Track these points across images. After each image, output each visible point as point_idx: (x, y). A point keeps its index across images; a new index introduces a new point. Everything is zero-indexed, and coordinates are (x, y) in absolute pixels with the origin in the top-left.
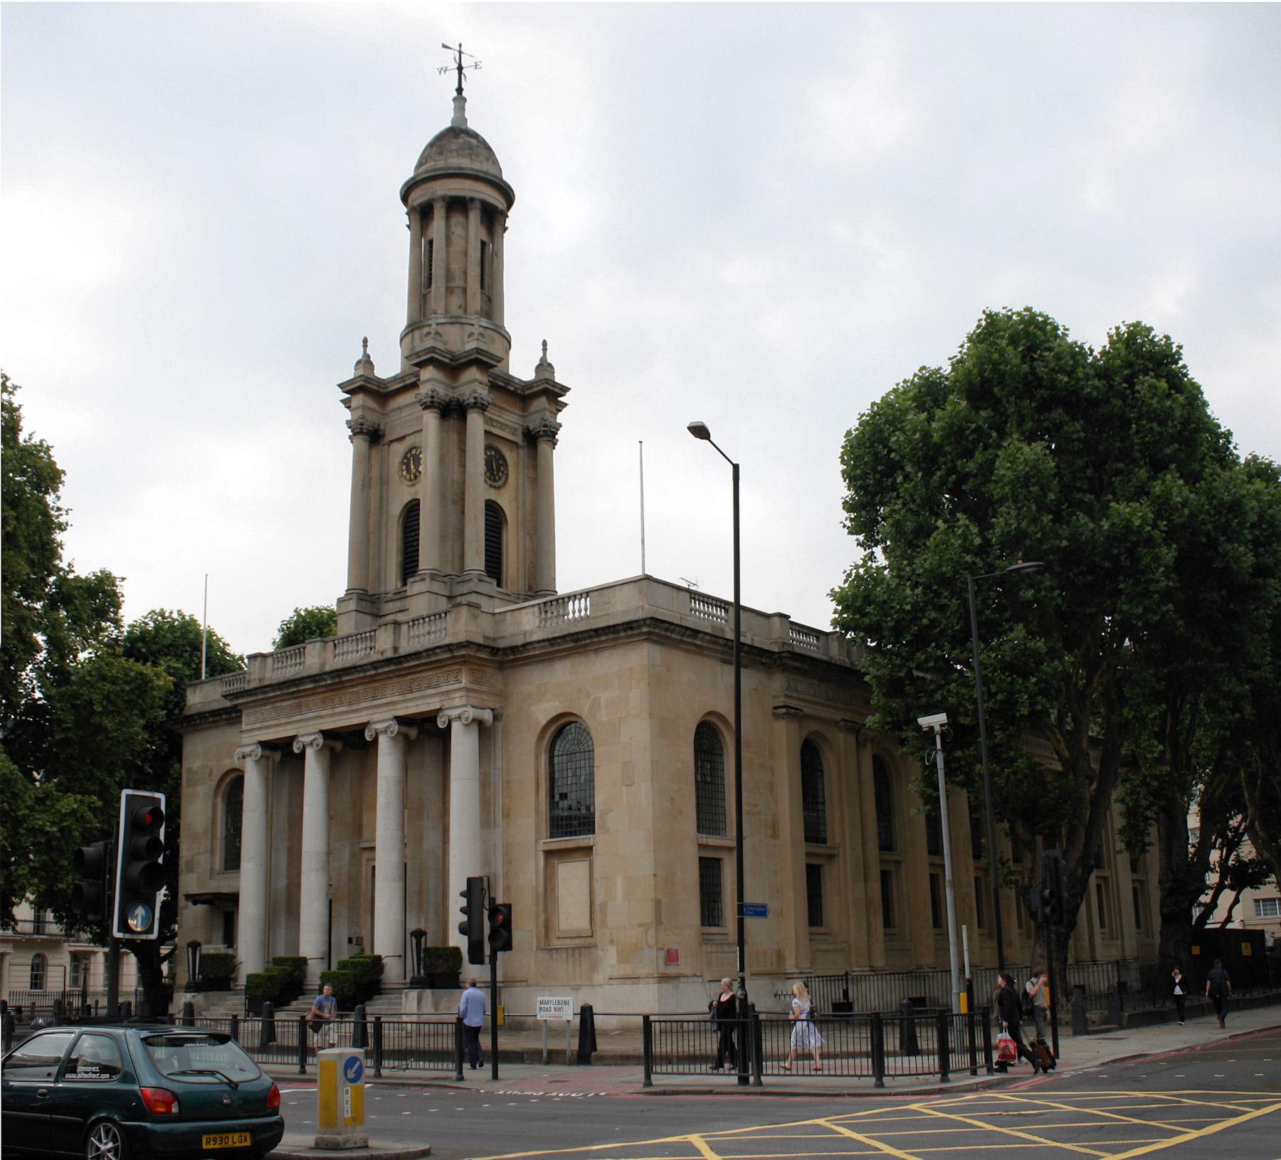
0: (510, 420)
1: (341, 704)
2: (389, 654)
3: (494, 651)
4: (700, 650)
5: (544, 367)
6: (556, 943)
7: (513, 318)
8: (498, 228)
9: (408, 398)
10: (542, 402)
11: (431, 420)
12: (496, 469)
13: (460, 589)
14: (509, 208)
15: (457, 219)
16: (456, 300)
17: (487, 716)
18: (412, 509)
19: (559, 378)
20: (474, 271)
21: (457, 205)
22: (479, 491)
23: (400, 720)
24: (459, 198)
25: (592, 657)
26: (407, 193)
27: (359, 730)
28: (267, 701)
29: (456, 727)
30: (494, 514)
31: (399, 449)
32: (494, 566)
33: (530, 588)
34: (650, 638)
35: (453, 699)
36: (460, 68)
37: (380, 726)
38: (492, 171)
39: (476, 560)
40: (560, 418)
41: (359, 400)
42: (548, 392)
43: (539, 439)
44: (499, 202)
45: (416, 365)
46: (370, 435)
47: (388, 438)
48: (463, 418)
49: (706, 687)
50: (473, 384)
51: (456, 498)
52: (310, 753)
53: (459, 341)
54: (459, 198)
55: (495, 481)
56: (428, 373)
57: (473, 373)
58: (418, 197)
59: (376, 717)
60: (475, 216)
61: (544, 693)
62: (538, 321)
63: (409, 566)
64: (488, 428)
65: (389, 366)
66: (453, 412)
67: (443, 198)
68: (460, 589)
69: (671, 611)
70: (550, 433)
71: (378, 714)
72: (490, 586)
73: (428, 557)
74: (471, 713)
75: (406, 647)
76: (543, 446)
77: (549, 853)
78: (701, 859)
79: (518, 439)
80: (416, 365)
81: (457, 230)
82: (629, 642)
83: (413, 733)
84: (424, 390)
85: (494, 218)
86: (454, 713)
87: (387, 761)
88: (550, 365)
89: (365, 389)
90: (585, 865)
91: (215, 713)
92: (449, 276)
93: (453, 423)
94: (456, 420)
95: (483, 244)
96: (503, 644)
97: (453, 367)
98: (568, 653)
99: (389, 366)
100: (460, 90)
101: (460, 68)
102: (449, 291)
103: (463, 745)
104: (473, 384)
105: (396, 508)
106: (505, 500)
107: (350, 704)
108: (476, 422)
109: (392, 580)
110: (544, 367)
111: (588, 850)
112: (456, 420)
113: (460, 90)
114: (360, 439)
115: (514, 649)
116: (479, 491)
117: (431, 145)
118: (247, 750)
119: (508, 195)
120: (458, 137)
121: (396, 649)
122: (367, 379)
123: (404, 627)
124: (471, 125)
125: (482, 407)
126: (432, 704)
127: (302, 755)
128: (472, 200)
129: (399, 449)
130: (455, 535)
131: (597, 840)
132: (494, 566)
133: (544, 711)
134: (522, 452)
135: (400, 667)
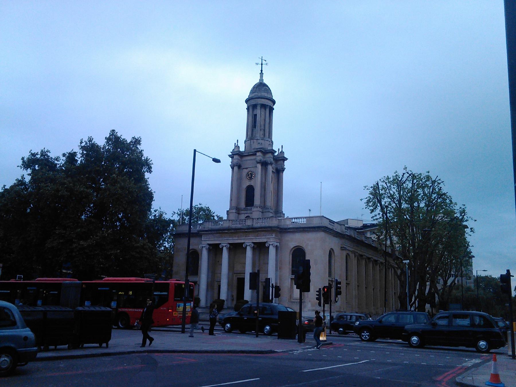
3: (281, 229)
4: (330, 234)
6: (293, 301)
11: (259, 166)
13: (265, 211)
17: (278, 244)
19: (286, 156)
21: (264, 106)
23: (254, 243)
27: (242, 244)
29: (271, 247)
31: (245, 172)
34: (324, 231)
35: (271, 240)
36: (262, 64)
37: (248, 244)
38: (269, 96)
42: (281, 159)
43: (279, 172)
47: (242, 167)
49: (334, 243)
51: (264, 188)
52: (224, 248)
57: (270, 155)
58: (253, 102)
59: (246, 242)
60: (268, 110)
61: (294, 241)
62: (280, 139)
65: (242, 149)
66: (265, 164)
68: (265, 211)
69: (326, 224)
70: (283, 169)
71: (248, 241)
74: (276, 244)
75: (255, 225)
76: (281, 174)
82: (317, 231)
83: (256, 246)
85: (271, 109)
87: (249, 253)
94: (258, 163)
96: (281, 227)
98: (300, 232)
100: (262, 71)
101: (262, 64)
102: (261, 130)
103: (272, 251)
109: (243, 205)
112: (258, 163)
113: (262, 71)
114: (236, 168)
115: (286, 229)
117: (254, 87)
118: (204, 246)
119: (274, 102)
123: (255, 220)
124: (265, 81)
125: (271, 164)
126: (264, 240)
128: (268, 105)
129: (245, 172)
130: (264, 196)
133: (292, 244)
134: (275, 174)
135: (254, 230)
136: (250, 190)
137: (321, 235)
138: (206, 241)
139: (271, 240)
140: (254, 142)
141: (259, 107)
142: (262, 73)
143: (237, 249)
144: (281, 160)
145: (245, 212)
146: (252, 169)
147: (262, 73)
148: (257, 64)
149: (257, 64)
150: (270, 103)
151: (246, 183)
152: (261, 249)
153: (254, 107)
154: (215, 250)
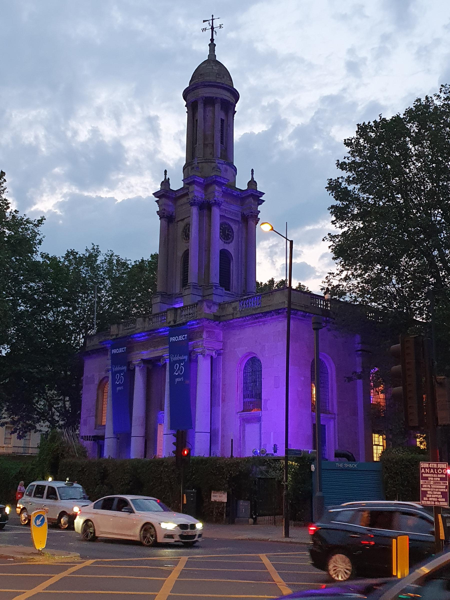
0: (233, 208)
2: (172, 323)
5: (252, 183)
7: (238, 160)
8: (230, 114)
9: (184, 200)
10: (251, 200)
11: (194, 210)
12: (226, 234)
14: (236, 103)
15: (209, 109)
16: (209, 150)
18: (186, 254)
20: (218, 135)
21: (209, 102)
22: (218, 244)
26: (186, 94)
30: (225, 256)
32: (225, 281)
33: (244, 291)
36: (212, 28)
38: (228, 83)
39: (215, 278)
40: (260, 208)
41: (163, 200)
42: (253, 195)
43: (250, 219)
44: (232, 100)
45: (187, 184)
46: (167, 217)
47: (176, 220)
48: (210, 210)
50: (216, 192)
51: (205, 247)
52: (137, 369)
53: (208, 170)
55: (227, 240)
56: (194, 188)
58: (192, 97)
60: (218, 107)
63: (185, 282)
64: (223, 214)
65: (177, 184)
66: (205, 207)
67: (202, 98)
72: (221, 291)
73: (192, 278)
76: (251, 223)
78: (45, 486)
79: (239, 219)
80: (187, 184)
81: (209, 115)
84: (190, 196)
88: (255, 182)
89: (165, 194)
90: (257, 426)
91: (97, 350)
92: (205, 138)
93: (206, 212)
95: (222, 121)
97: (207, 184)
99: (177, 184)
100: (212, 40)
101: (212, 28)
102: (205, 145)
104: (216, 192)
105: (180, 254)
106: (231, 248)
108: (216, 211)
110: (252, 183)
111: (259, 419)
113: (212, 40)
116: (218, 244)
119: (236, 96)
121: (175, 321)
122: (167, 192)
123: (179, 311)
125: (218, 204)
128: (216, 98)
129: (181, 225)
131: (264, 414)
132: (225, 281)
133: (240, 351)
137: (278, 327)
142: (212, 46)
144: (248, 196)
147: (212, 46)
150: (227, 96)
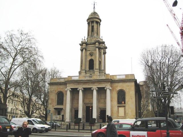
1: (87, 85)
11: (97, 49)
13: (101, 72)
24: (94, 22)
25: (126, 83)
28: (72, 83)
35: (108, 86)
36: (94, 4)
37: (94, 88)
38: (98, 17)
47: (87, 50)
54: (94, 22)
56: (97, 43)
58: (92, 20)
59: (93, 87)
66: (100, 49)
68: (101, 72)
77: (118, 106)
86: (108, 88)
94: (93, 48)
100: (94, 7)
101: (94, 4)
103: (108, 92)
107: (88, 85)
109: (88, 69)
111: (125, 106)
112: (93, 48)
113: (94, 7)
117: (92, 14)
120: (95, 13)
124: (96, 12)
127: (79, 91)
129: (88, 52)
136: (91, 62)
138: (69, 87)
139: (108, 86)
140: (93, 38)
141: (95, 23)
143: (87, 91)
145: (89, 72)
146: (92, 51)
148: (92, 4)
149: (92, 4)
150: (99, 21)
151: (89, 58)
152: (102, 91)
153: (92, 22)
154: (74, 92)
